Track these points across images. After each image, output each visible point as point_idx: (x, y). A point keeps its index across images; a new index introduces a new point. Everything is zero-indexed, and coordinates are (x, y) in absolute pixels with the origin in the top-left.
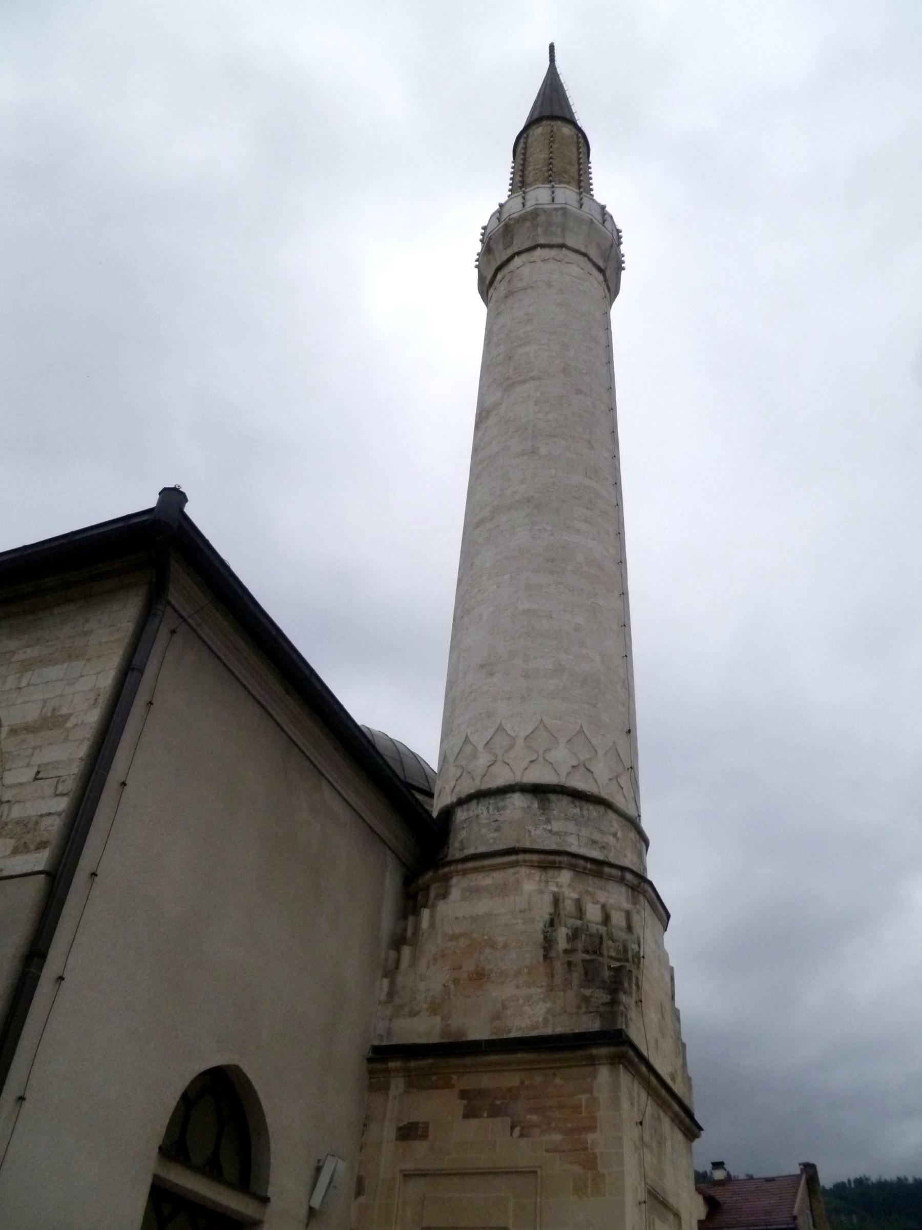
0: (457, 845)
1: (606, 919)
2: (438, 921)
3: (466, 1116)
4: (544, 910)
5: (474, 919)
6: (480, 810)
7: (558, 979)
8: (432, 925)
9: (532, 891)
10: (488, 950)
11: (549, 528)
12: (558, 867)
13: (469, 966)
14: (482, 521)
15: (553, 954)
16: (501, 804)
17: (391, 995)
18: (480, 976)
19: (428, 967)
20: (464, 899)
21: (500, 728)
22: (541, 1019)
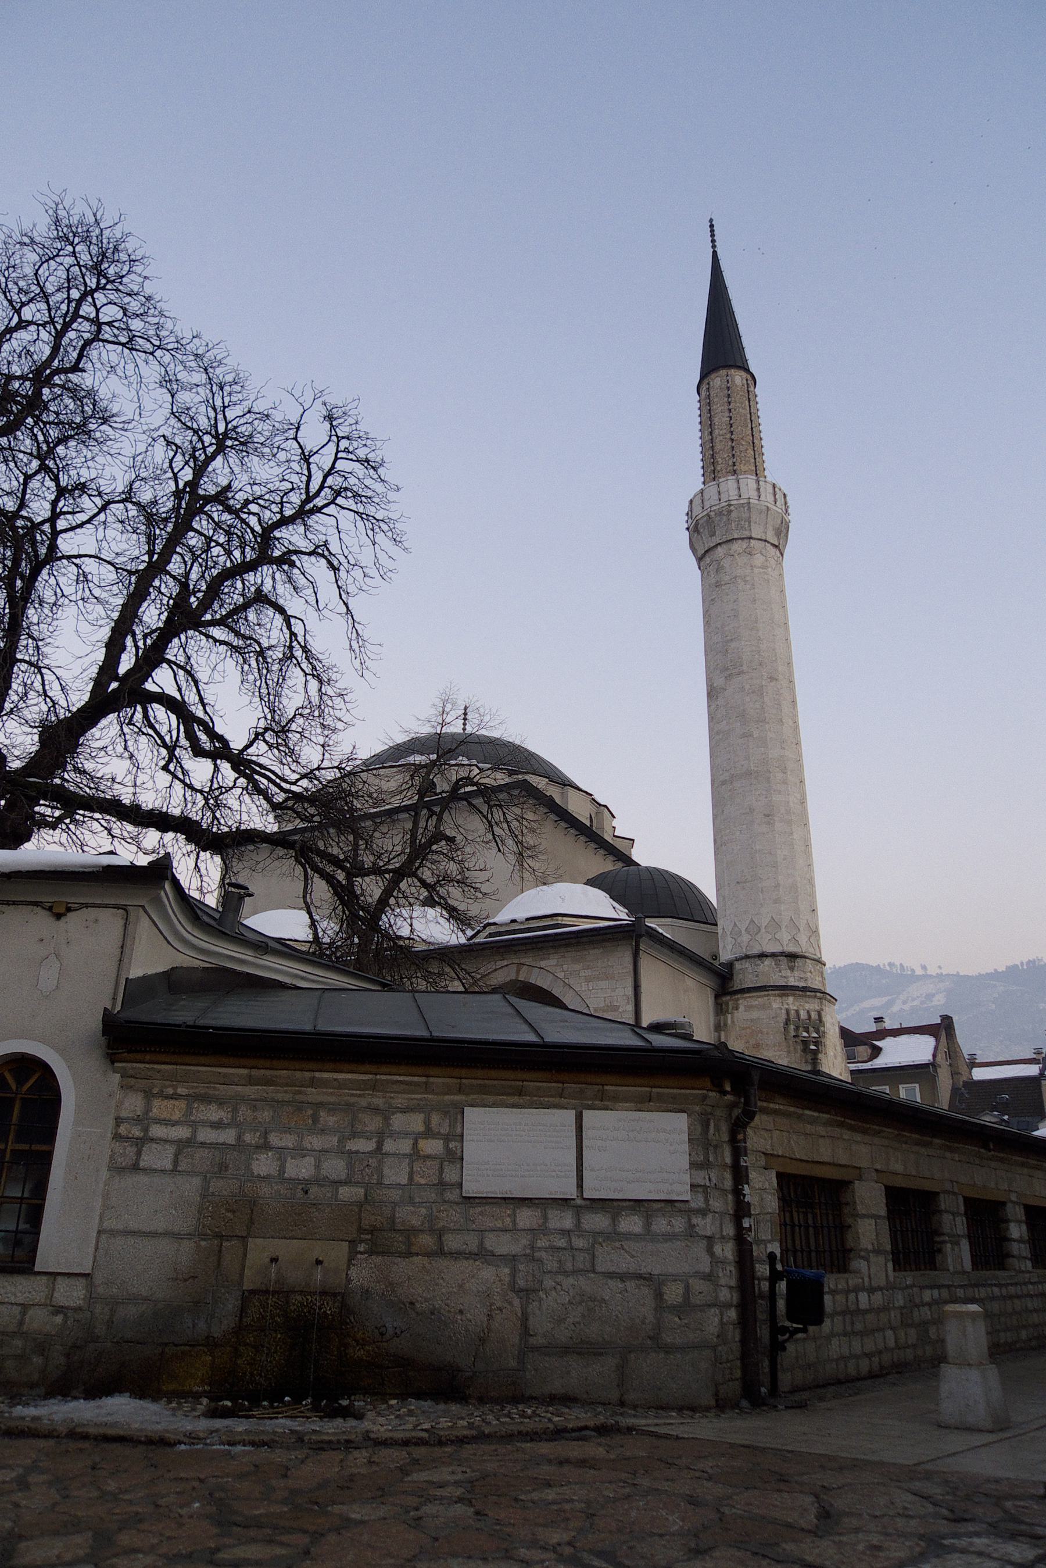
1: (810, 1017)
4: (784, 1016)
5: (752, 1020)
6: (746, 964)
7: (792, 1048)
8: (733, 1022)
9: (777, 1004)
13: (752, 1042)
14: (724, 783)
21: (752, 921)
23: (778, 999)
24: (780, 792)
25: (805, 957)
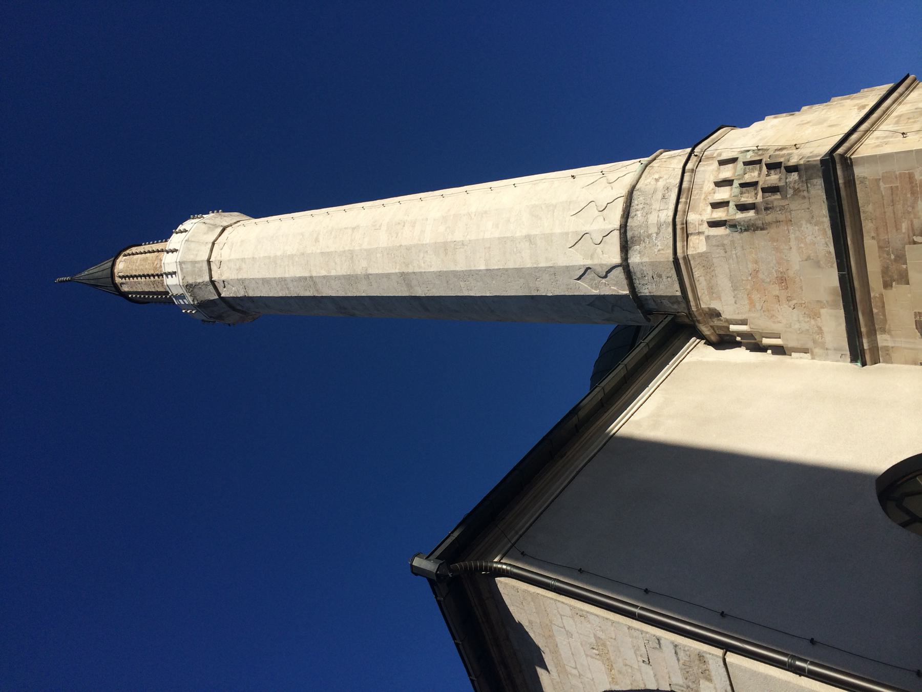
0: (675, 306)
1: (727, 183)
2: (739, 317)
3: (908, 284)
5: (735, 288)
7: (781, 217)
8: (744, 322)
10: (761, 276)
11: (422, 255)
12: (686, 224)
13: (775, 290)
15: (759, 223)
16: (639, 275)
17: (806, 351)
18: (783, 280)
19: (779, 322)
20: (719, 298)
22: (817, 228)
23: (693, 239)
24: (423, 232)
25: (633, 188)
